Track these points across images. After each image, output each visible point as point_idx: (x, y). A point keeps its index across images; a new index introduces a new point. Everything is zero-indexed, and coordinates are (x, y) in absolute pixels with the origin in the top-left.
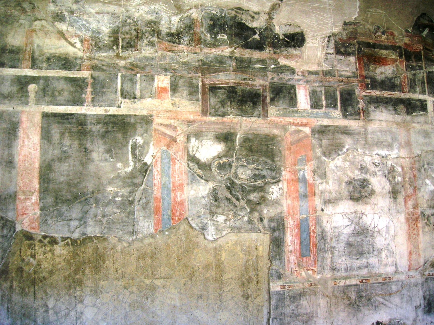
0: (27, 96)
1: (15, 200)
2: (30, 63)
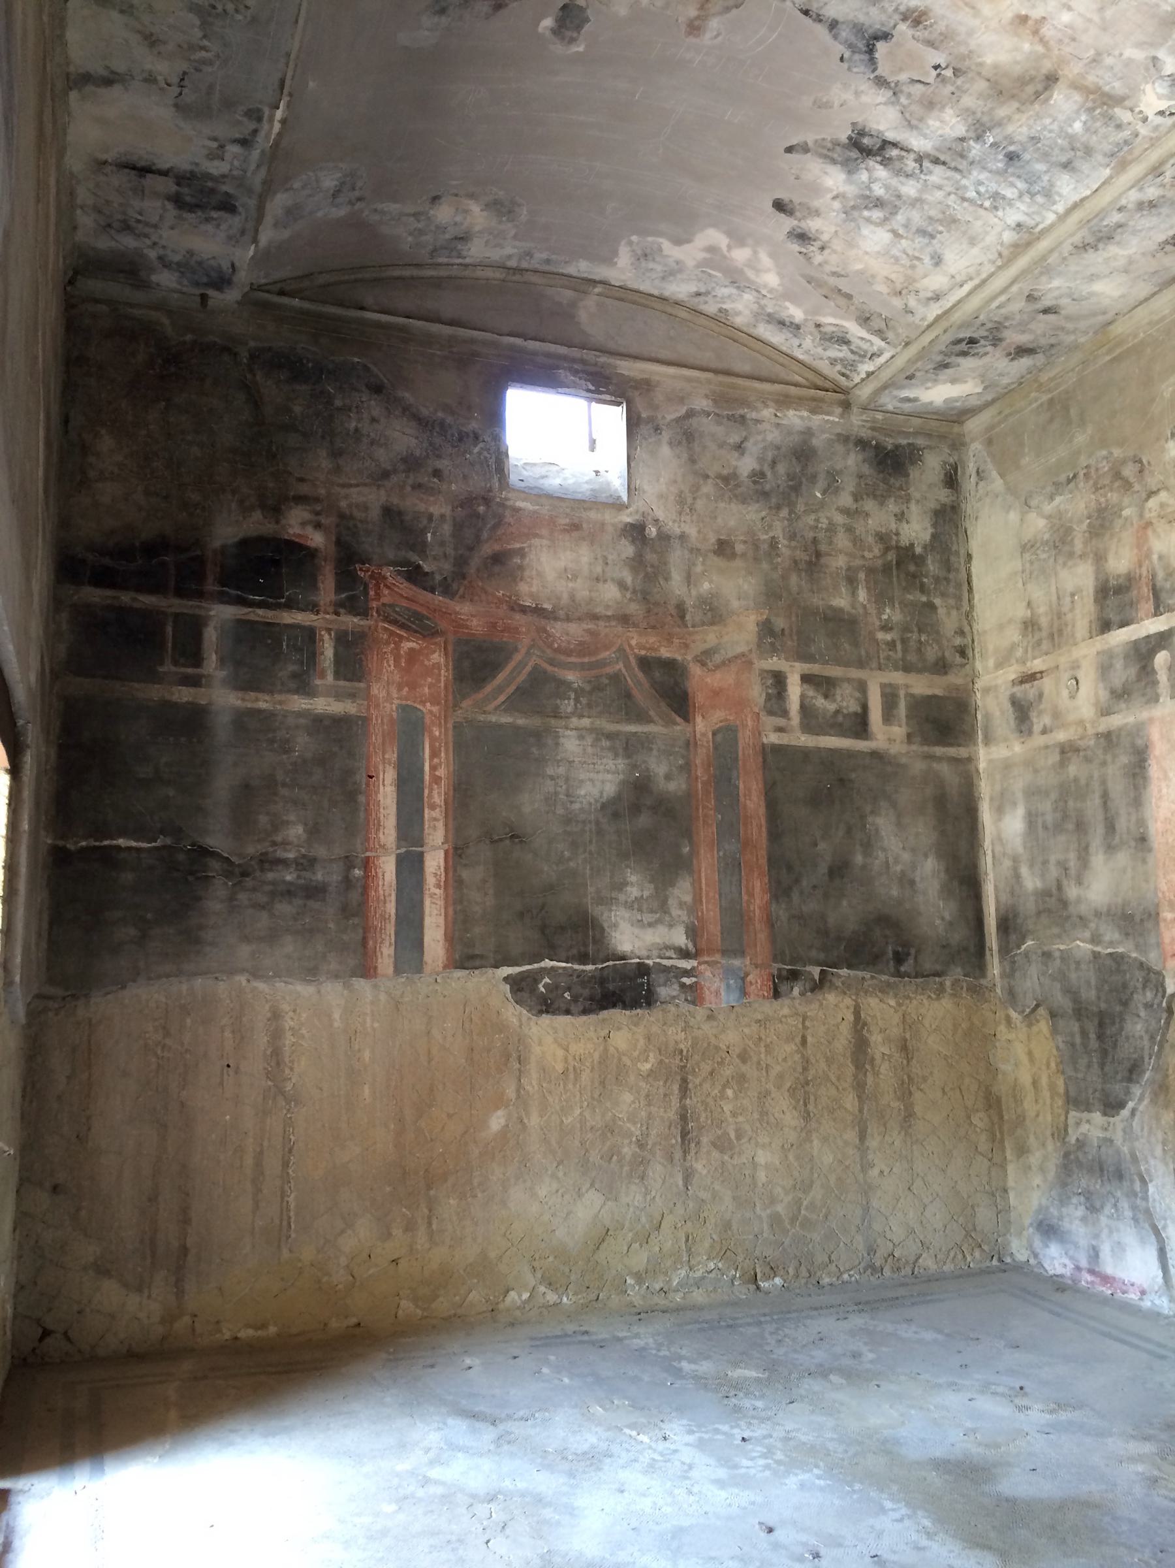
0: (1155, 683)
1: (1157, 923)
2: (1150, 606)
